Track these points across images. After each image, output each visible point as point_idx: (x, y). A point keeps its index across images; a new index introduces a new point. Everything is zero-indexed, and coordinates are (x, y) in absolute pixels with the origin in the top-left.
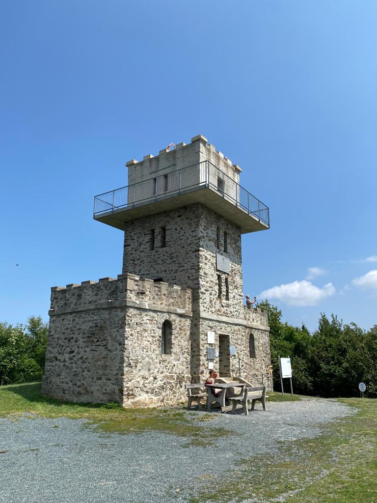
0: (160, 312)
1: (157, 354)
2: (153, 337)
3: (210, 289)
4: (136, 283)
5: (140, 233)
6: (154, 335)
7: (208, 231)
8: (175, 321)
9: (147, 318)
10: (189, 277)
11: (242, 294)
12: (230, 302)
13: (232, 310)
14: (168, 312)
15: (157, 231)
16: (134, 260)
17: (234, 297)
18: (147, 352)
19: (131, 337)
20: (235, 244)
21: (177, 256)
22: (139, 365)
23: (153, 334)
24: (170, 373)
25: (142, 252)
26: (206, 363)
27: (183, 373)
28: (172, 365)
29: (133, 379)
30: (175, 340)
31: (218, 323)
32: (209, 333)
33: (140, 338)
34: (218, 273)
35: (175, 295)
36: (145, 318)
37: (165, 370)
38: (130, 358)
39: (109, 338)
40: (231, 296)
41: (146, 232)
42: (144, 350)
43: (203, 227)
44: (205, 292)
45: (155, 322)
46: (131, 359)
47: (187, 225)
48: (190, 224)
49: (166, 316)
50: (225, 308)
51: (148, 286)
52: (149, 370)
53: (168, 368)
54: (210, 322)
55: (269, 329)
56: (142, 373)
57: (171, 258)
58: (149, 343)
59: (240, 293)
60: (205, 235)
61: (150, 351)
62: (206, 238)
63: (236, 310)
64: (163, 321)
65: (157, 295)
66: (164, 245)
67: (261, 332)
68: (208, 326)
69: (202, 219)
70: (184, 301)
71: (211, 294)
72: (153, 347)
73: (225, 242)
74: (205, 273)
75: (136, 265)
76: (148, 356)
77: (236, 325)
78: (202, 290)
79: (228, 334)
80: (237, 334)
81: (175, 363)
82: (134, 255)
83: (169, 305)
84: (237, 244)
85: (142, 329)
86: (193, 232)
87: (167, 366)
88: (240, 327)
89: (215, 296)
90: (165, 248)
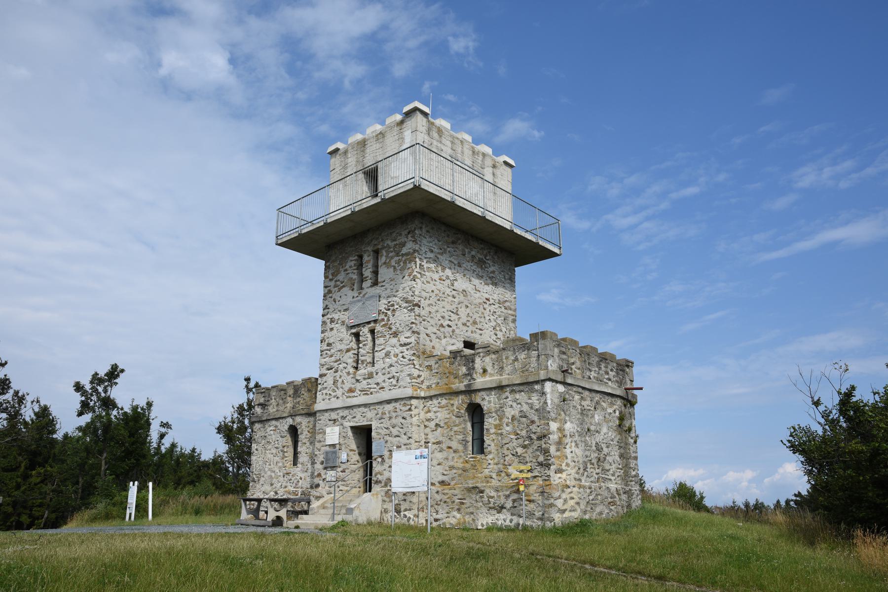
2: (277, 448)
3: (336, 364)
17: (387, 355)
18: (270, 465)
22: (262, 479)
23: (276, 445)
24: (294, 488)
26: (323, 472)
28: (298, 478)
30: (301, 447)
32: (328, 430)
34: (354, 331)
37: (288, 484)
46: (255, 474)
49: (290, 421)
52: (272, 485)
53: (292, 481)
58: (272, 455)
67: (512, 391)
68: (330, 420)
77: (389, 402)
79: (369, 423)
80: (390, 418)
87: (291, 480)
88: (397, 405)
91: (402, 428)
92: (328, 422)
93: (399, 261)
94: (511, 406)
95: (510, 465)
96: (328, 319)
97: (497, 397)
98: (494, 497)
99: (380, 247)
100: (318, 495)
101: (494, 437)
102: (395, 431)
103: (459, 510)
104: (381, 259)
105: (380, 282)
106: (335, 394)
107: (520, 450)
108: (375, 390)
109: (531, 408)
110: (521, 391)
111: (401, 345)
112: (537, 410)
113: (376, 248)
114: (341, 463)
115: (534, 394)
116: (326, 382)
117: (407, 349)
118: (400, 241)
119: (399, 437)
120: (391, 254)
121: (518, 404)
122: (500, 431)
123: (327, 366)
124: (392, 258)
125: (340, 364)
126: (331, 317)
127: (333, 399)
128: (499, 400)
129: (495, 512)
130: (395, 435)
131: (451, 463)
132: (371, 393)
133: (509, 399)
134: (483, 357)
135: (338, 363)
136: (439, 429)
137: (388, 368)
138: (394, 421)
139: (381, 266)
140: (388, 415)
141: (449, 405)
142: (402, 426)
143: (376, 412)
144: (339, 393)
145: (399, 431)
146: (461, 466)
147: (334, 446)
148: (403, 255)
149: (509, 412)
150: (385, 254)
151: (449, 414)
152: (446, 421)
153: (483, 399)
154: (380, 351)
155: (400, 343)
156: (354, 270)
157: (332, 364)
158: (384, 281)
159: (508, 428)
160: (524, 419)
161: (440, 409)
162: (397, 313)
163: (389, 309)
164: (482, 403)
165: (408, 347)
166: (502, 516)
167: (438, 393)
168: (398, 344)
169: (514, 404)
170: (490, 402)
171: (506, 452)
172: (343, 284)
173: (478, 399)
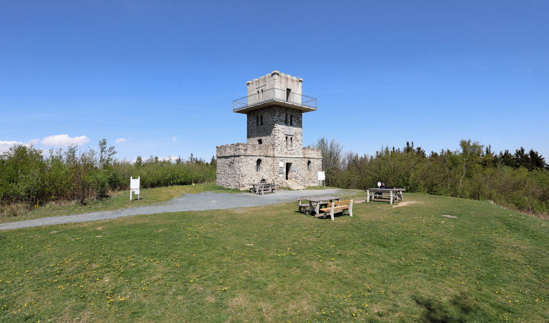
0: (255, 156)
3: (281, 144)
4: (244, 146)
5: (253, 118)
7: (280, 117)
8: (263, 159)
10: (271, 139)
11: (302, 144)
12: (294, 148)
13: (294, 152)
15: (259, 117)
16: (251, 130)
17: (296, 145)
20: (298, 120)
21: (267, 130)
22: (246, 177)
25: (254, 127)
26: (278, 175)
27: (268, 179)
31: (285, 158)
32: (280, 163)
33: (246, 167)
34: (286, 136)
35: (263, 148)
36: (248, 159)
39: (235, 167)
40: (293, 145)
41: (255, 118)
43: (277, 116)
44: (278, 145)
45: (253, 160)
47: (270, 115)
48: (271, 115)
49: (259, 158)
50: (290, 151)
51: (250, 146)
52: (251, 178)
54: (281, 158)
55: (322, 157)
56: (248, 179)
57: (264, 131)
59: (300, 143)
60: (278, 120)
62: (279, 121)
63: (297, 151)
64: (257, 159)
65: (254, 149)
66: (262, 124)
67: (316, 160)
69: (277, 112)
70: (268, 150)
71: (281, 146)
73: (291, 120)
74: (278, 137)
75: (252, 133)
76: (250, 173)
77: (297, 158)
78: (276, 145)
80: (297, 162)
81: (264, 175)
82: (251, 128)
83: (260, 153)
84: (299, 120)
86: (272, 118)
88: (299, 159)
89: (284, 147)
90: (262, 126)
99: (293, 115)
100: (277, 181)
102: (298, 165)
103: (307, 183)
127: (281, 154)
131: (306, 173)
144: (283, 153)
146: (307, 174)
147: (281, 167)
162: (298, 136)
173: (310, 160)
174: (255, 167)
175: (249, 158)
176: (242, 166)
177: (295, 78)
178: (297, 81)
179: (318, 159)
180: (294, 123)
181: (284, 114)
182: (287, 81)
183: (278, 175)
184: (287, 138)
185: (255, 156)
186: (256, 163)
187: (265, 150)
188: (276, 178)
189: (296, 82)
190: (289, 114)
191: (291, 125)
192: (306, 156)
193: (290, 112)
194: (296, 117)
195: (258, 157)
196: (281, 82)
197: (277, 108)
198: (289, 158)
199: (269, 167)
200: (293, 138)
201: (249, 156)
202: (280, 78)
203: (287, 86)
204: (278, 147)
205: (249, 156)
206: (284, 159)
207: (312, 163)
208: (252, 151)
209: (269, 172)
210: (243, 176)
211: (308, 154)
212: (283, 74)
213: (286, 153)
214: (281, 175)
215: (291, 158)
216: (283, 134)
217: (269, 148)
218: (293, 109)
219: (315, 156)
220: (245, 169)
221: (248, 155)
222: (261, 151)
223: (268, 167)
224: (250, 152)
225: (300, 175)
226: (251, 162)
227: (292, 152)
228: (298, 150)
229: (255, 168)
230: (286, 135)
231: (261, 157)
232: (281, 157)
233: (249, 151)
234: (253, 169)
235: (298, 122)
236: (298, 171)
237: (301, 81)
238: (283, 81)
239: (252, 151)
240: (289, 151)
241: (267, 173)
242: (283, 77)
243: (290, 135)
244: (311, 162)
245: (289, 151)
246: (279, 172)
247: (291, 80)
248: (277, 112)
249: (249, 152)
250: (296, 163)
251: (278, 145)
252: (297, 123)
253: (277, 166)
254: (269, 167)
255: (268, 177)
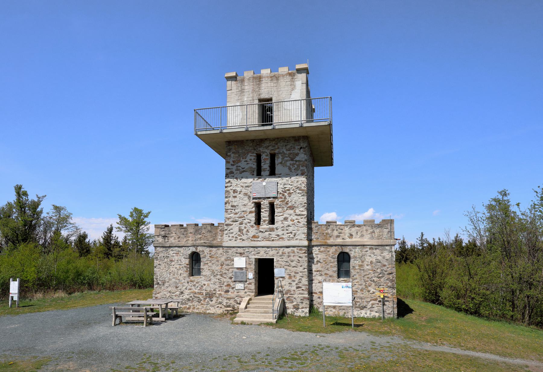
0: (185, 247)
1: (185, 277)
3: (240, 219)
4: (163, 229)
6: (181, 263)
7: (239, 164)
9: (173, 252)
14: (194, 246)
17: (286, 219)
18: (174, 275)
19: (159, 266)
20: (292, 160)
22: (166, 284)
23: (179, 263)
24: (199, 290)
27: (215, 290)
29: (161, 292)
30: (204, 265)
33: (167, 266)
35: (204, 231)
36: (171, 253)
37: (193, 287)
38: (158, 279)
42: (171, 274)
44: (232, 223)
45: (181, 254)
46: (159, 280)
49: (193, 249)
50: (267, 233)
51: (174, 230)
52: (177, 287)
54: (239, 249)
56: (169, 289)
58: (176, 269)
60: (234, 170)
61: (178, 275)
65: (183, 234)
67: (370, 249)
68: (236, 253)
70: (216, 234)
71: (241, 224)
72: (180, 272)
74: (232, 206)
76: (174, 278)
77: (288, 247)
79: (272, 258)
80: (289, 256)
81: (206, 283)
83: (195, 240)
85: (168, 260)
88: (295, 249)
89: (248, 224)
91: (299, 263)
92: (235, 254)
93: (293, 165)
94: (370, 256)
95: (369, 286)
96: (231, 190)
97: (360, 250)
98: (359, 302)
99: (276, 151)
100: (229, 297)
101: (358, 271)
102: (293, 264)
104: (277, 160)
105: (277, 174)
106: (241, 237)
107: (375, 279)
108: (277, 239)
109: (384, 258)
110: (376, 249)
111: (296, 215)
112: (387, 260)
113: (272, 152)
114: (248, 279)
115: (386, 251)
116: (232, 229)
117: (302, 218)
118: (294, 151)
119: (297, 267)
120: (286, 159)
121: (375, 255)
122: (362, 268)
123: (232, 220)
124: (287, 161)
125: (245, 219)
126: (234, 189)
127: (239, 240)
128: (361, 251)
129: (359, 309)
130: (293, 266)
132: (273, 240)
133: (369, 252)
134: (350, 228)
135: (243, 219)
136: (319, 264)
137: (287, 227)
138: (292, 258)
139: (277, 165)
140: (287, 254)
141: (327, 251)
142: (299, 262)
143: (277, 251)
144: (244, 237)
145: (296, 264)
147: (241, 269)
148: (296, 161)
149: (368, 259)
150: (281, 157)
151: (326, 256)
152: (324, 260)
153: (350, 250)
154: (279, 216)
155: (296, 213)
156: (254, 162)
157: (237, 219)
158: (281, 174)
159: (368, 267)
160: (379, 264)
161: (319, 253)
162: (293, 196)
163: (286, 192)
164: (350, 253)
165: (302, 217)
166: (363, 312)
167: (319, 244)
168: (294, 214)
169: (372, 255)
170: (355, 252)
171: (367, 279)
172: (244, 169)
173: (346, 250)
174: (185, 267)
175: (173, 251)
176: (159, 264)
177: (283, 70)
178: (290, 74)
179: (381, 248)
180: (279, 168)
181: (250, 154)
182: (259, 84)
183: (232, 284)
184: (258, 206)
185: (185, 247)
186: (187, 261)
187: (208, 234)
188: (227, 291)
189: (289, 78)
190: (263, 152)
191: (272, 173)
192: (331, 241)
193: (267, 147)
194: (285, 154)
195: (191, 248)
196: (242, 91)
197: (231, 147)
198: (263, 247)
199: (217, 268)
200: (275, 203)
201: (170, 247)
202: (239, 85)
203: (260, 95)
204: (231, 227)
205: (170, 247)
206: (247, 250)
207: (355, 257)
208: (179, 238)
209: (219, 277)
210: (160, 283)
211: (338, 237)
212: (248, 74)
213: (254, 236)
214: (240, 286)
215: (268, 247)
216: (246, 198)
217: (219, 230)
218: (278, 138)
219: (366, 240)
220: (164, 270)
221: (169, 245)
222: (200, 236)
223: (216, 268)
224: (175, 239)
225: (298, 288)
226: (176, 258)
227: (273, 234)
228: (291, 229)
229: (185, 269)
230: (254, 199)
231: (199, 248)
232: (239, 247)
233: (173, 238)
234: (180, 272)
235: (293, 165)
236: (290, 277)
237: (299, 71)
238: (246, 87)
239: (179, 238)
240: (262, 232)
241: (214, 280)
242: (249, 79)
243: (269, 198)
244: (352, 256)
245: (262, 232)
246: (233, 279)
247: (270, 79)
248: (232, 155)
249: (172, 240)
250: (285, 258)
251: (233, 221)
252: (290, 169)
253: (230, 267)
254: (217, 268)
255: (217, 287)
